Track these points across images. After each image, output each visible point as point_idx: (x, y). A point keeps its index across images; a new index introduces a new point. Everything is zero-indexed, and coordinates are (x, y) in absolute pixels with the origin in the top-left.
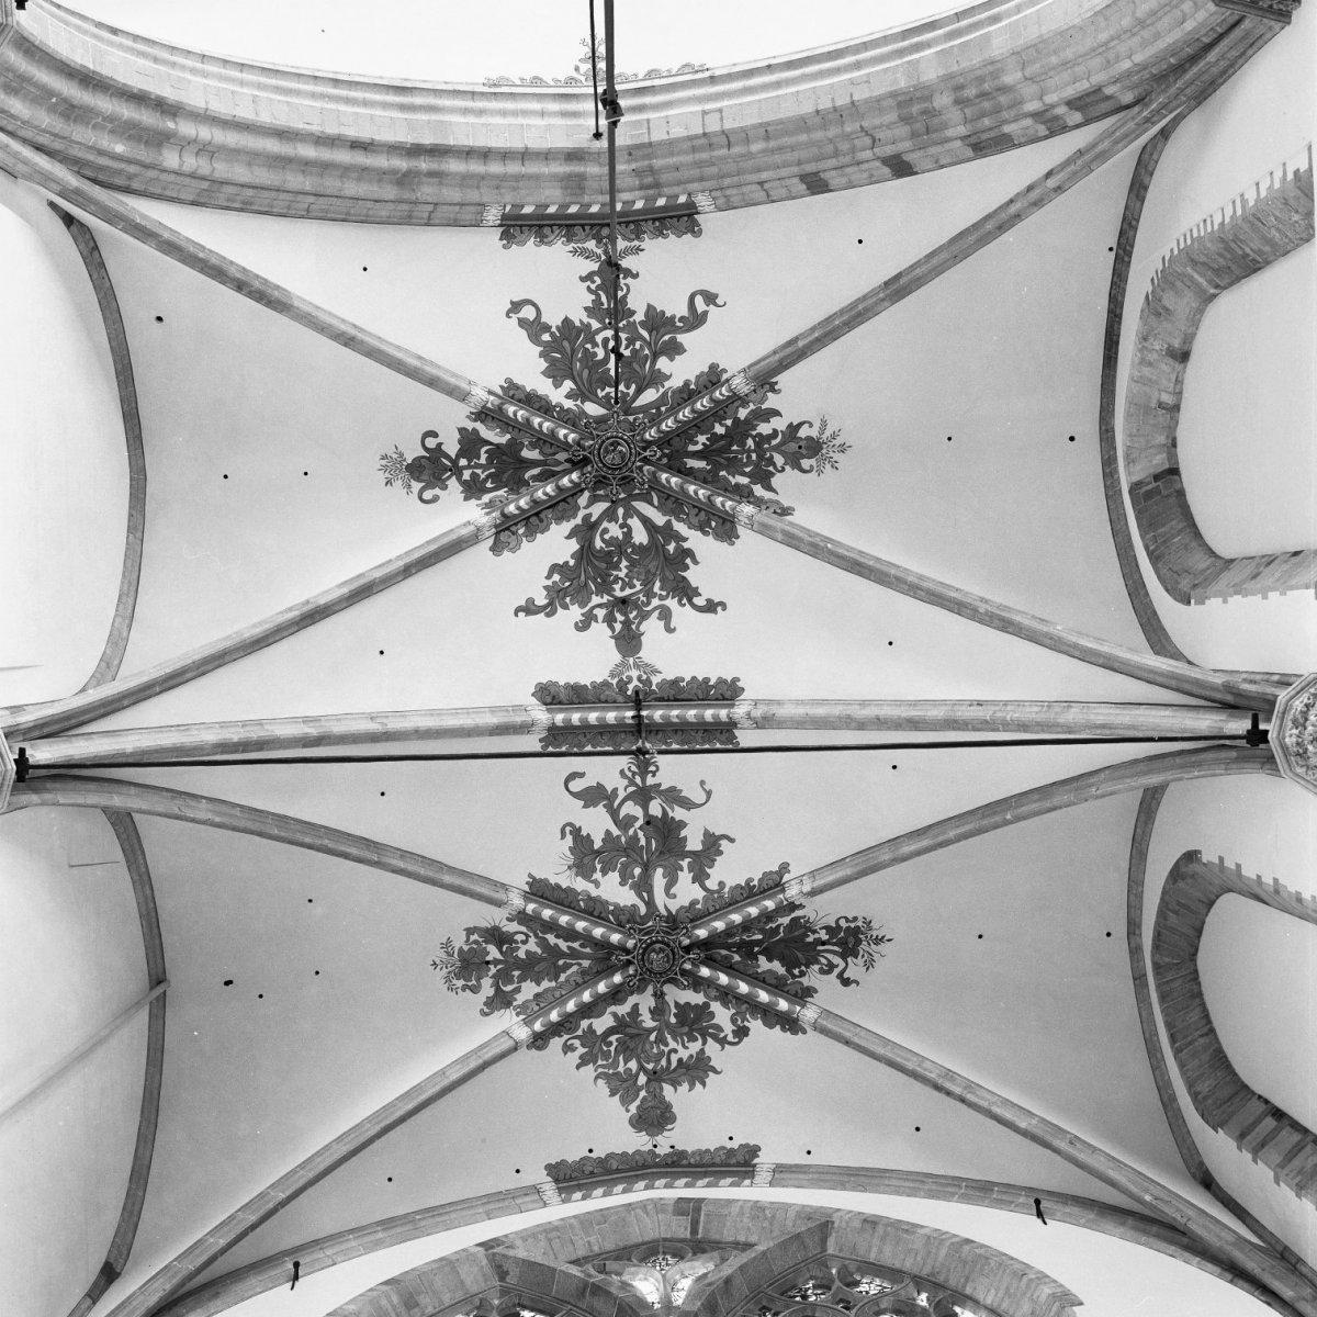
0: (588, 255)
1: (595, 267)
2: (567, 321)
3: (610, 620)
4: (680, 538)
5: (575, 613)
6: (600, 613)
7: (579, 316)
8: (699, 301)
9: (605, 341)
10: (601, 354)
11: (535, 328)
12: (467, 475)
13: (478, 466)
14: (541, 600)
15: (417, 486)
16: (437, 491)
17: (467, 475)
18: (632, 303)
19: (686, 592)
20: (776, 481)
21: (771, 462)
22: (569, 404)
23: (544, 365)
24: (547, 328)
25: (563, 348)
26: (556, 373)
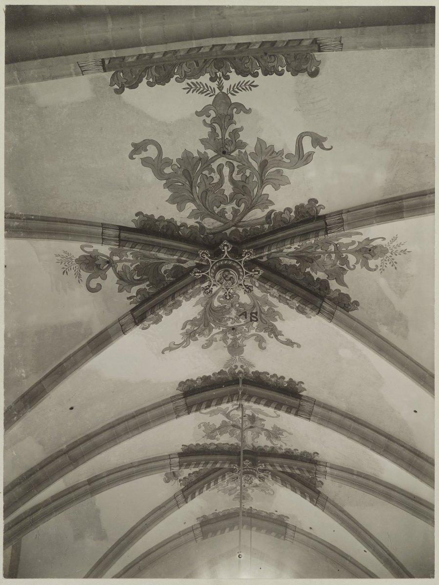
0: (203, 90)
1: (210, 100)
2: (187, 155)
3: (224, 339)
4: (271, 305)
5: (202, 340)
6: (218, 337)
7: (196, 148)
8: (307, 142)
9: (220, 167)
10: (216, 178)
11: (158, 165)
12: (119, 267)
13: (126, 261)
14: (179, 340)
15: (85, 275)
16: (99, 280)
17: (119, 269)
18: (243, 137)
19: (274, 332)
20: (347, 278)
21: (345, 261)
22: (191, 222)
23: (168, 193)
24: (168, 162)
25: (186, 176)
26: (177, 200)
